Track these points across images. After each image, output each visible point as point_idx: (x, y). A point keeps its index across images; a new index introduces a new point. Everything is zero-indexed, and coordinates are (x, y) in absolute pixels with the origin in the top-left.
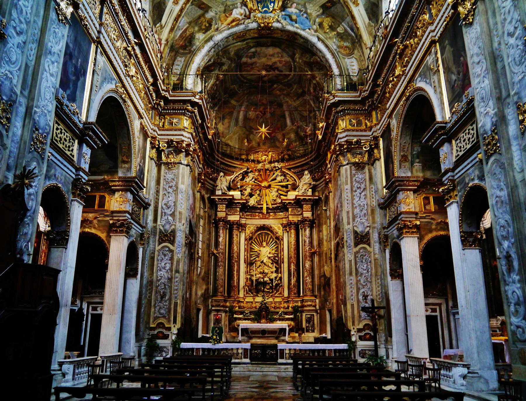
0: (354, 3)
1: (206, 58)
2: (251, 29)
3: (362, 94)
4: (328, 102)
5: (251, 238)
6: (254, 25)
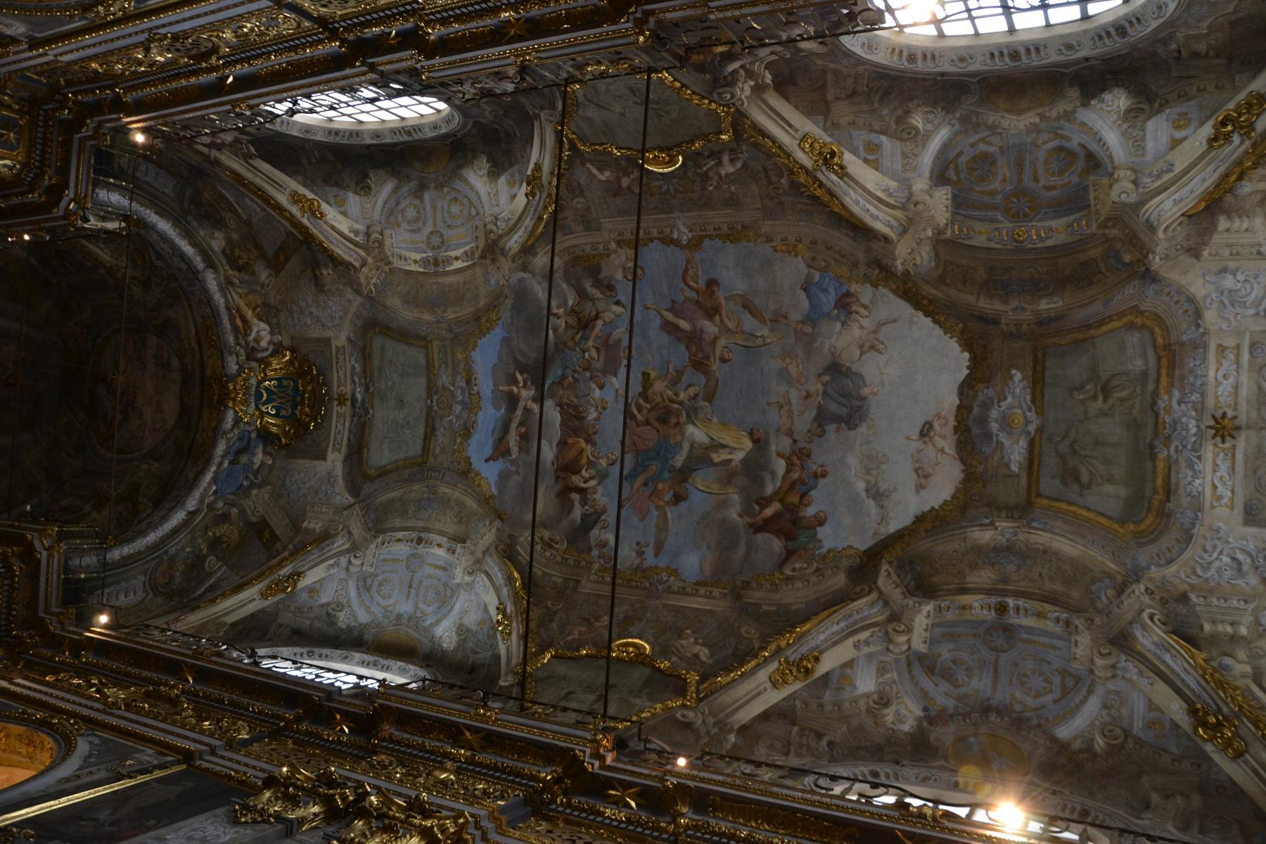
0: (269, 588)
1: (166, 247)
2: (223, 360)
3: (55, 619)
4: (36, 534)
6: (233, 367)
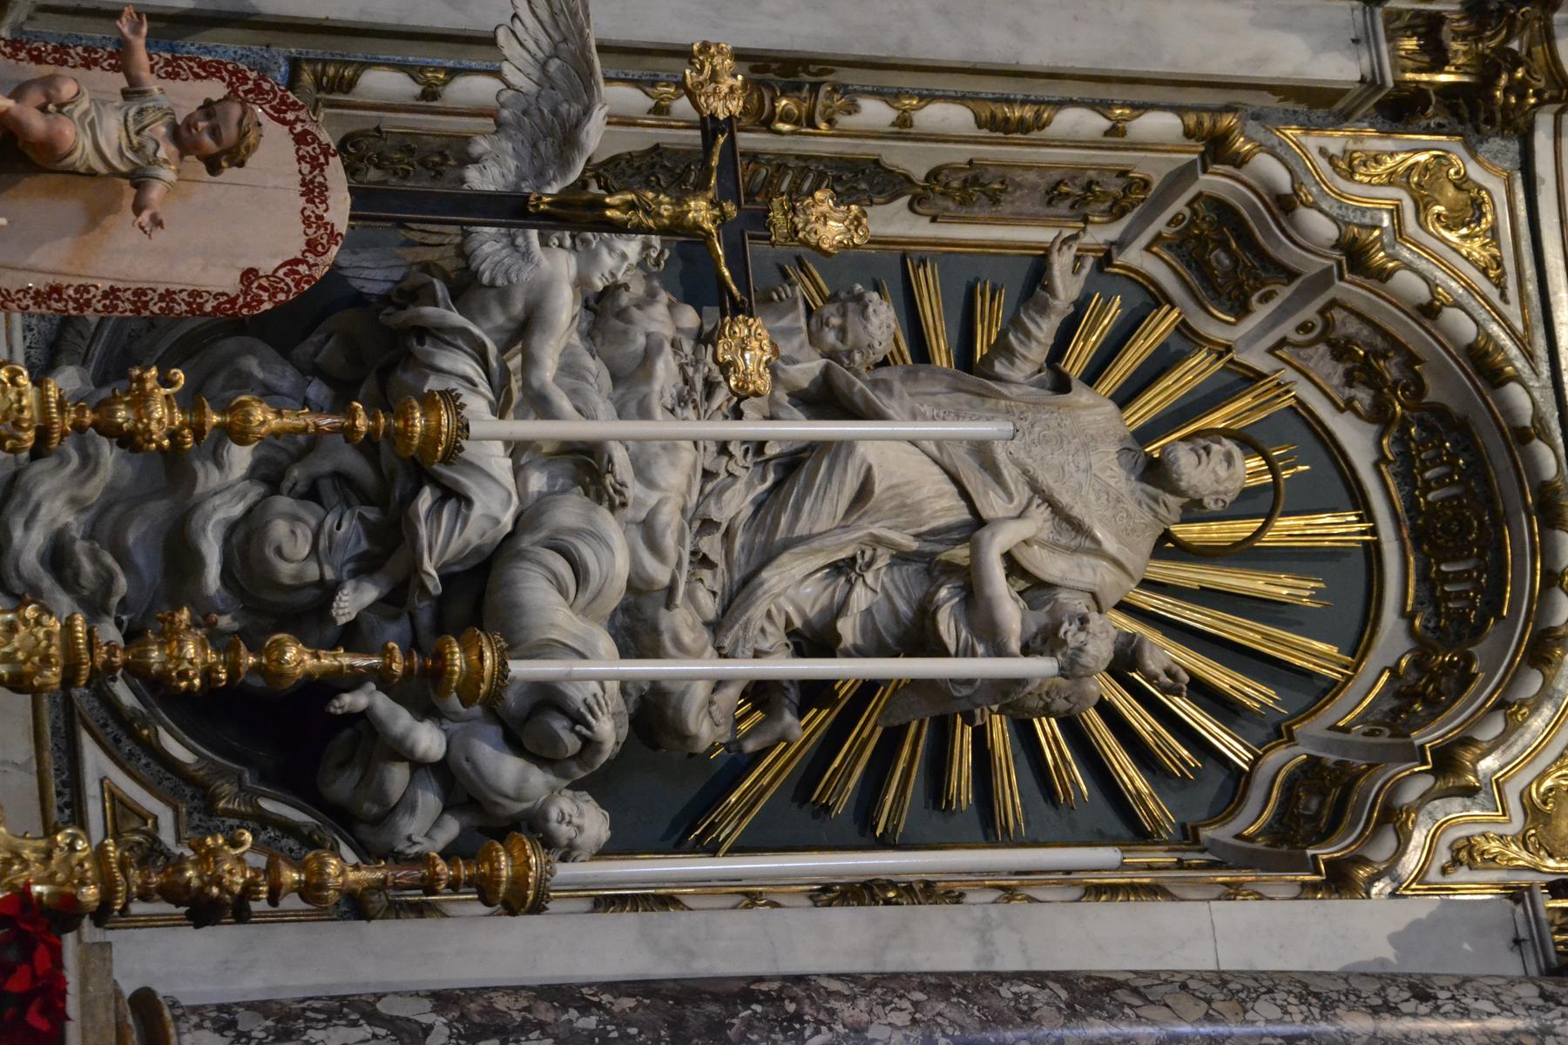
5: (1231, 253)
